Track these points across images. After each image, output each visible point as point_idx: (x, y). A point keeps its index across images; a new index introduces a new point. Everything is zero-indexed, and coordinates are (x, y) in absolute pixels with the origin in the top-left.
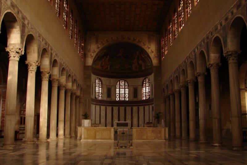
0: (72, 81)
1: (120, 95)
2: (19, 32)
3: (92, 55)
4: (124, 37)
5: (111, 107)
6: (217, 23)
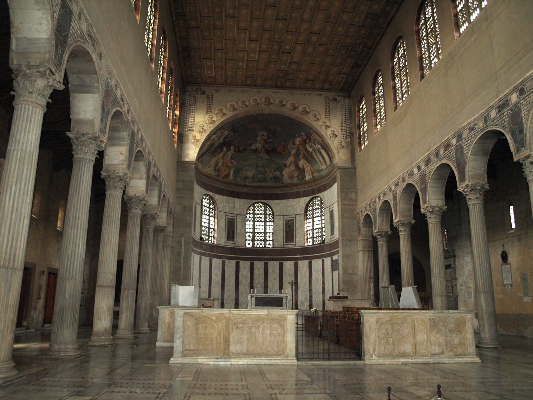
1: (254, 236)
3: (198, 137)
4: (272, 101)
5: (234, 262)
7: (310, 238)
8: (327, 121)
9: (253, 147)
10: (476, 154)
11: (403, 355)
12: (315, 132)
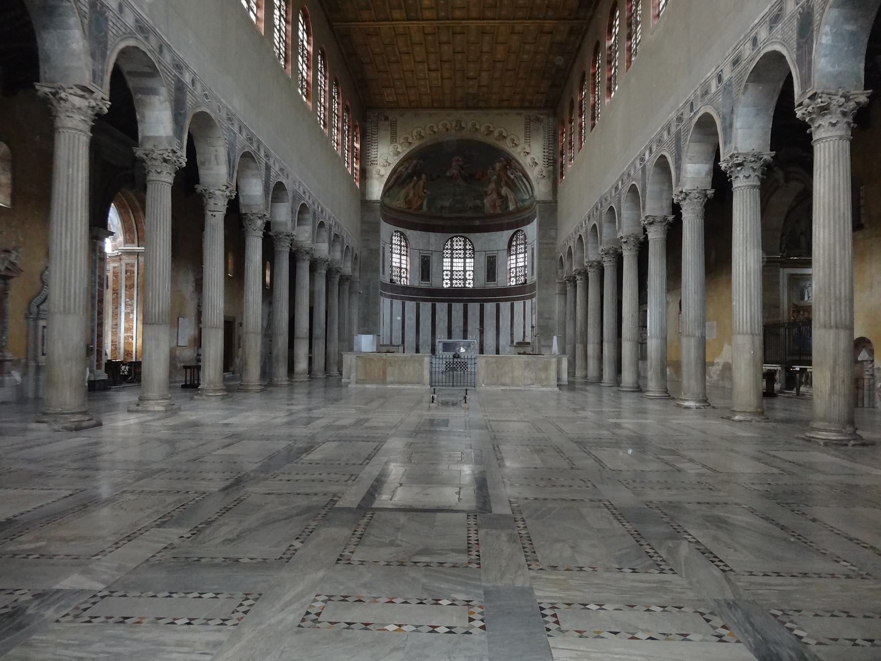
0: (330, 239)
1: (452, 275)
2: (167, 104)
5: (429, 305)
6: (709, 74)
7: (513, 277)
8: (526, 146)
9: (448, 174)
10: (610, 222)
11: (504, 385)
12: (513, 159)
